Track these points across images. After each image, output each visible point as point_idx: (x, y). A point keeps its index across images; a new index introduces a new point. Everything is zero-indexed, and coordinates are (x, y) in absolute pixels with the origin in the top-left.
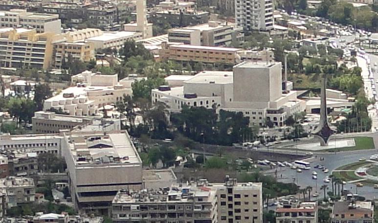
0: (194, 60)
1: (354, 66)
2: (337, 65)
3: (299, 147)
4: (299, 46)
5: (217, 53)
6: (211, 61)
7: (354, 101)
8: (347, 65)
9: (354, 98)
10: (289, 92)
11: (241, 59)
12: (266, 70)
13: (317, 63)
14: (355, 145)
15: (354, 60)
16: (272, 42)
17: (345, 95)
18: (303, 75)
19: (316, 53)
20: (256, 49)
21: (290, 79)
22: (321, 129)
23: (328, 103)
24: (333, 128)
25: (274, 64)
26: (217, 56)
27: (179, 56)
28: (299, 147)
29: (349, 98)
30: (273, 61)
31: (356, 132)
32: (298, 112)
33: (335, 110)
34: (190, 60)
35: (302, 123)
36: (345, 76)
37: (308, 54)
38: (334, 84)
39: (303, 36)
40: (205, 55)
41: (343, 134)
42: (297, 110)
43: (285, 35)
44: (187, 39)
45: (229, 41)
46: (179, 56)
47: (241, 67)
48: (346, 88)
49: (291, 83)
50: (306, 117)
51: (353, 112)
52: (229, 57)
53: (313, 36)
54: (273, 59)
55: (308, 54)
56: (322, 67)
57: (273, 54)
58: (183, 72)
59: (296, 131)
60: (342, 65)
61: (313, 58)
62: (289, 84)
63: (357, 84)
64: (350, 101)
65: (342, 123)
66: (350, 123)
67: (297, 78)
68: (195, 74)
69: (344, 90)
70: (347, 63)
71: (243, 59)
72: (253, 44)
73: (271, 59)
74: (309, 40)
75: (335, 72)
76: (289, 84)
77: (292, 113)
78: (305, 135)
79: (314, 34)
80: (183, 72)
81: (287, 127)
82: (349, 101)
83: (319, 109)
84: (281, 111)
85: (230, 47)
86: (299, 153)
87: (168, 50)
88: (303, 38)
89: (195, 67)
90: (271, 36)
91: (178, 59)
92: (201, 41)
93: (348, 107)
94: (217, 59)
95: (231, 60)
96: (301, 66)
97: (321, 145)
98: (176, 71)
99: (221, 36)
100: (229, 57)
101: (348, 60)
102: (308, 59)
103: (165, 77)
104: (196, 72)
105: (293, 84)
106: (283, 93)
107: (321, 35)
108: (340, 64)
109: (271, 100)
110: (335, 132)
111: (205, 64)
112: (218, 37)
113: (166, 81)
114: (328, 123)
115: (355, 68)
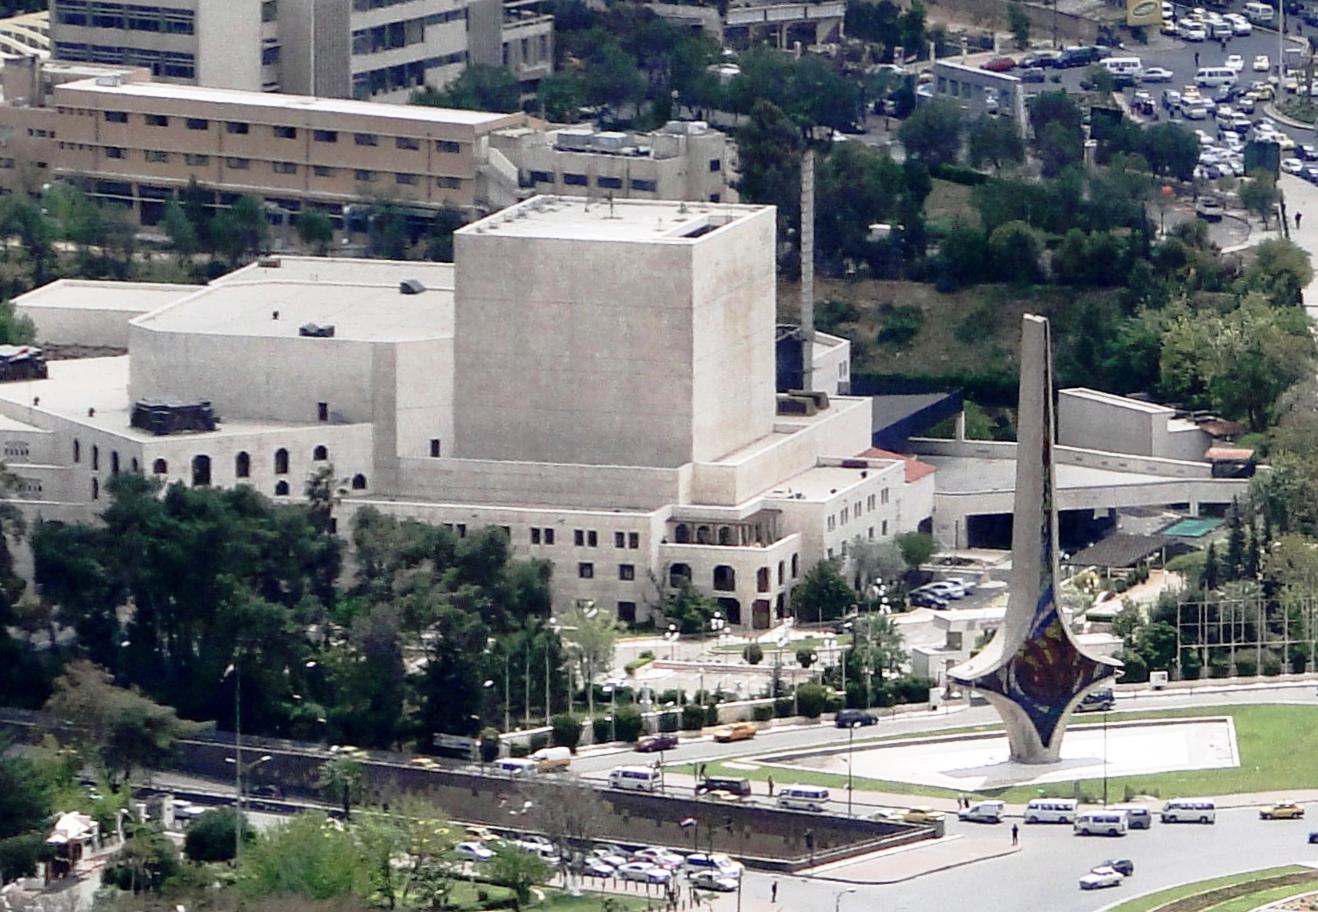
0: (212, 184)
1: (1257, 238)
2: (1149, 231)
3: (865, 764)
4: (906, 102)
5: (365, 140)
6: (322, 191)
7: (1249, 469)
8: (1214, 234)
9: (1246, 453)
10: (819, 401)
11: (522, 184)
12: (677, 259)
13: (1020, 214)
14: (1237, 763)
15: (1262, 202)
16: (730, 71)
17: (1192, 426)
18: (920, 294)
19: (1013, 149)
20: (626, 112)
21: (833, 319)
22: (1017, 646)
23: (1066, 476)
24: (1096, 645)
25: (729, 220)
26: (363, 158)
27: (116, 153)
28: (865, 764)
29: (1218, 452)
30: (733, 194)
31: (1246, 670)
32: (878, 537)
33: (1127, 525)
34: (185, 181)
35: (899, 607)
36: (1194, 307)
37: (963, 154)
38: (1124, 357)
39: (939, 34)
40: (288, 151)
41: (1160, 692)
42: (871, 519)
43: (823, 32)
44: (174, 42)
45: (453, 59)
46: (116, 153)
47: (505, 231)
48: (1197, 386)
49: (845, 345)
50: (925, 567)
51: (1236, 540)
52: (445, 165)
53: (1003, 36)
54: (732, 185)
55: (963, 154)
56: (1051, 245)
57: (728, 153)
58: (138, 257)
59: (851, 667)
60: (1183, 231)
61: (998, 182)
62: (829, 359)
63: (1273, 363)
64: (1222, 469)
65: (1156, 618)
66: (1213, 610)
67: (887, 308)
68: (216, 271)
69: (1186, 397)
70: (1216, 219)
71: (534, 180)
72: (606, 80)
73: (714, 182)
74: (972, 63)
75: (1132, 277)
76: (829, 359)
77: (833, 540)
78: (915, 692)
79: (1014, 29)
80: (138, 257)
81: (801, 635)
82: (1215, 474)
83: (1008, 519)
84: (763, 528)
85: (455, 100)
86: (865, 807)
87: (44, 117)
88: (941, 52)
89: (215, 233)
90: (735, 34)
91: (112, 171)
92: (270, 56)
93: (1211, 510)
94: (363, 174)
95: (453, 182)
96: (914, 236)
97: (1017, 758)
98: (96, 250)
99: (398, 27)
100: (445, 165)
101: (1222, 203)
102: (964, 191)
103: (19, 289)
104: (221, 258)
105: (855, 352)
106: (784, 408)
107: (1057, 32)
108: (1167, 220)
109: (701, 454)
110: (1109, 671)
111: (286, 212)
112: (378, 31)
113: (18, 314)
114: (1066, 614)
115: (1266, 254)
